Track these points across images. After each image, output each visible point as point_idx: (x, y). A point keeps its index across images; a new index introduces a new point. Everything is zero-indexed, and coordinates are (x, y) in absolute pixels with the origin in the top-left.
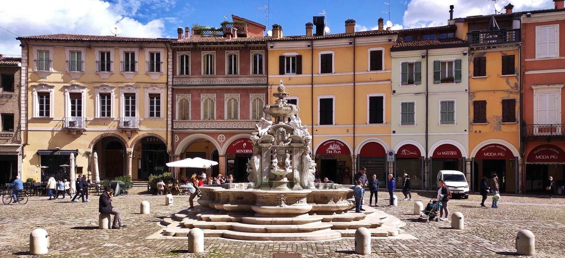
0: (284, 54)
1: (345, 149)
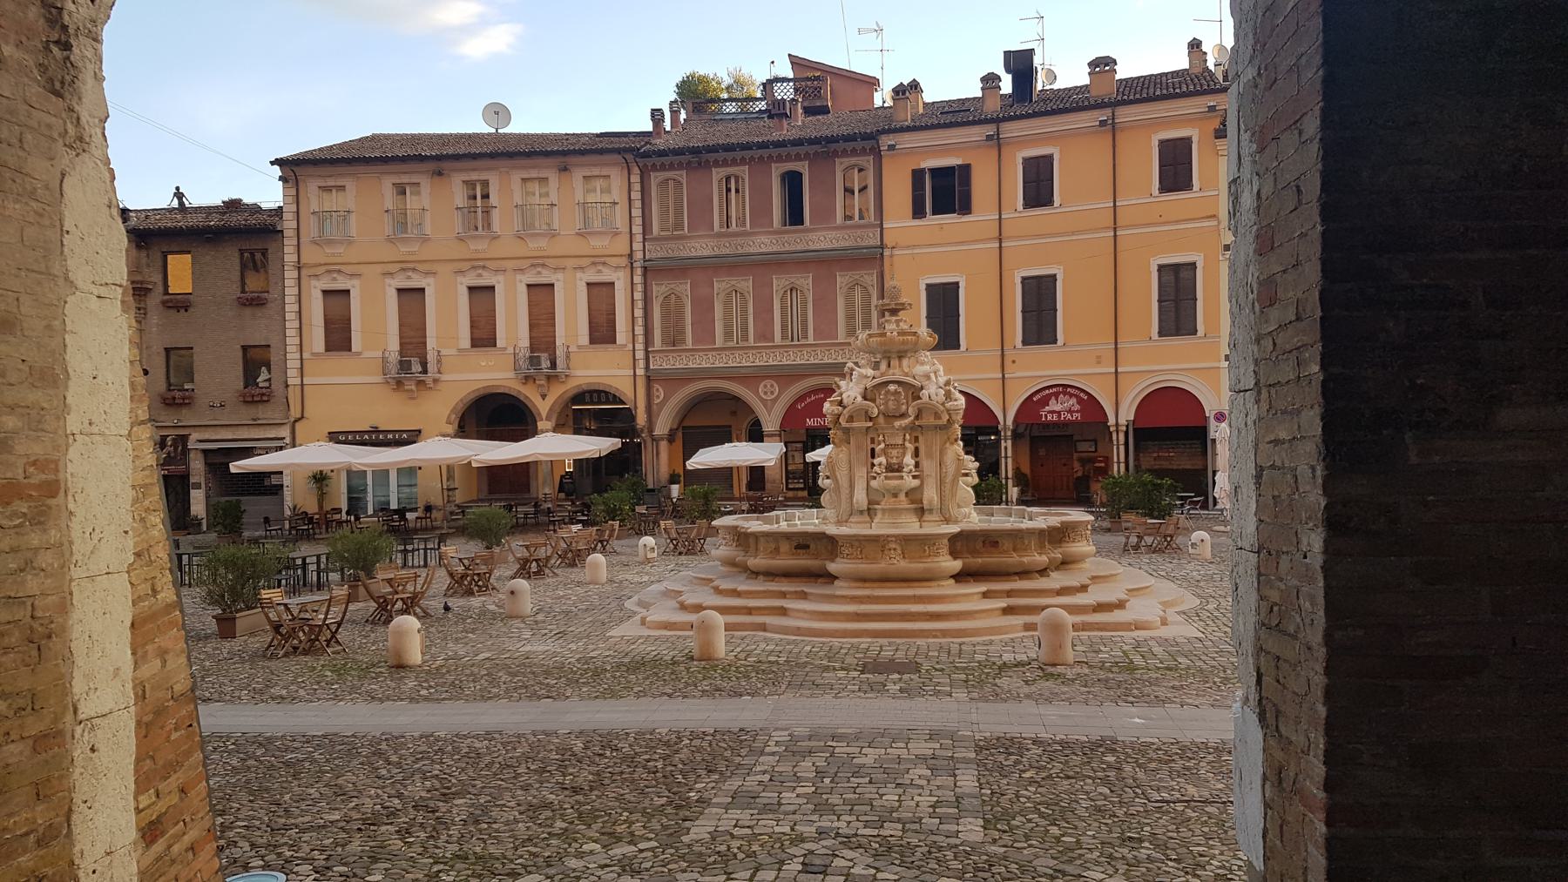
0: (923, 165)
1: (1090, 404)
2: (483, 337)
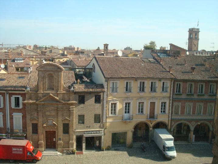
2: (141, 111)
